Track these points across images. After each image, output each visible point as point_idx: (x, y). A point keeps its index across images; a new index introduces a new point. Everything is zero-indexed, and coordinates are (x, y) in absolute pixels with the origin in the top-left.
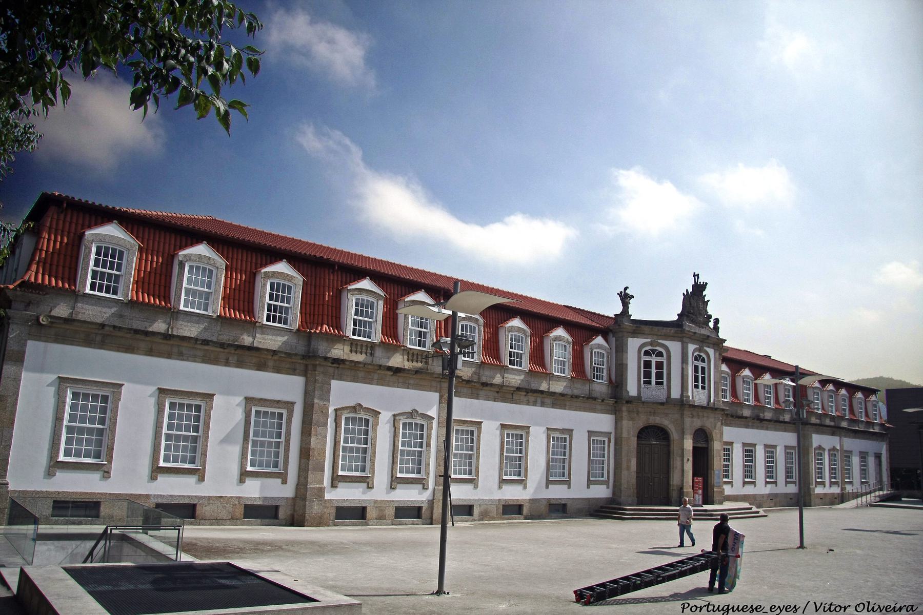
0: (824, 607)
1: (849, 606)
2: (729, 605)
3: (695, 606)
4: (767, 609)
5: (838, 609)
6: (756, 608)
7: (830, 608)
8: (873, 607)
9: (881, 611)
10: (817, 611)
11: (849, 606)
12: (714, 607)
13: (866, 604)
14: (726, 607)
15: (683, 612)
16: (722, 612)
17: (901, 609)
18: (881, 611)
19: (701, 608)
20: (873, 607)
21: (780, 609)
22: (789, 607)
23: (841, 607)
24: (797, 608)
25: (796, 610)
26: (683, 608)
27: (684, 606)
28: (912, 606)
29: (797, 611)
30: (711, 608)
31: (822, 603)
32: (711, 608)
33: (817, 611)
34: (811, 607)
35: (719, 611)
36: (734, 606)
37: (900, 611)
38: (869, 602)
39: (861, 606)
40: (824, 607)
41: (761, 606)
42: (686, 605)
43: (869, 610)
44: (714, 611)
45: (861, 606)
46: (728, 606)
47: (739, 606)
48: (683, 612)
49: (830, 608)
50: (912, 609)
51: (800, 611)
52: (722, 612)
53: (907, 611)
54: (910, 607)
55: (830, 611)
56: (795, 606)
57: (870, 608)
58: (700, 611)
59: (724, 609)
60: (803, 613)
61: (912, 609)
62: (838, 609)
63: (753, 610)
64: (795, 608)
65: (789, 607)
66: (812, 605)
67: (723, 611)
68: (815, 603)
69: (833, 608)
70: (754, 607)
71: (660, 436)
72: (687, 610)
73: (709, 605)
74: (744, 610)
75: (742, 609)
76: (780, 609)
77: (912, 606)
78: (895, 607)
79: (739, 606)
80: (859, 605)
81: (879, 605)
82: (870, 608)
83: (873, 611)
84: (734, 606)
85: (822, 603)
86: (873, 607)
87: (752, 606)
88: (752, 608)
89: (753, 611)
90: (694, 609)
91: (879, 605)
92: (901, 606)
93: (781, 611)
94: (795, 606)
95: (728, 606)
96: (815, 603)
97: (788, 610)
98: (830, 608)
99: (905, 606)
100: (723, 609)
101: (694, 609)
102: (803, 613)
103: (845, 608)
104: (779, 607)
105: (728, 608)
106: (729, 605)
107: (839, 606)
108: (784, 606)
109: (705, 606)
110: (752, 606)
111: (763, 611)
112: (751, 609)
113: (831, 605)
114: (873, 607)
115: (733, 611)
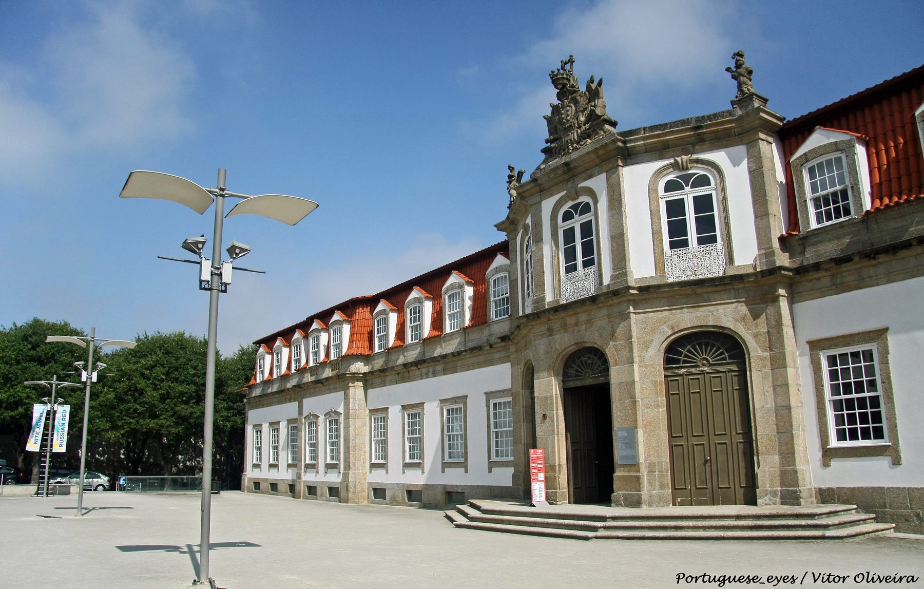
0: (823, 578)
1: (849, 576)
2: (725, 576)
3: (690, 576)
4: (764, 580)
5: (837, 579)
6: (753, 579)
7: (829, 578)
8: (873, 578)
9: (881, 582)
10: (815, 581)
11: (849, 576)
12: (710, 577)
13: (866, 575)
14: (722, 578)
15: (678, 583)
16: (718, 583)
17: (901, 579)
18: (881, 582)
19: (697, 579)
20: (873, 578)
21: (778, 579)
22: (786, 578)
23: (840, 578)
24: (795, 578)
25: (794, 581)
26: (679, 579)
27: (679, 576)
28: (913, 577)
29: (794, 582)
30: (706, 578)
31: (820, 574)
32: (706, 578)
33: (815, 581)
34: (809, 578)
35: (715, 582)
36: (730, 577)
37: (900, 582)
38: (868, 573)
39: (861, 576)
40: (823, 578)
41: (758, 577)
42: (682, 576)
43: (869, 580)
44: (709, 582)
45: (861, 576)
46: (725, 576)
47: (735, 576)
48: (678, 583)
49: (828, 579)
50: (912, 579)
51: (798, 581)
52: (718, 583)
53: (908, 582)
54: (910, 578)
55: (829, 582)
56: (793, 576)
57: (870, 579)
58: (696, 582)
59: (721, 580)
60: (801, 584)
61: (912, 579)
62: (837, 579)
63: (750, 580)
64: (793, 579)
65: (786, 578)
66: (809, 576)
67: (720, 581)
68: (813, 573)
69: (831, 578)
70: (750, 578)
71: (686, 356)
72: (683, 581)
73: (705, 575)
74: (741, 581)
75: (739, 580)
76: (778, 579)
77: (913, 577)
78: (895, 578)
80: (858, 575)
81: (878, 576)
82: (870, 579)
83: (873, 582)
84: (730, 577)
85: (820, 574)
86: (873, 578)
87: (749, 576)
88: (749, 579)
89: (750, 582)
90: (689, 579)
91: (878, 576)
92: (901, 577)
93: (778, 582)
94: (793, 576)
95: (725, 576)
96: (813, 573)
97: (785, 581)
98: (828, 579)
99: (906, 576)
100: (719, 580)
101: (689, 579)
102: (801, 584)
103: (844, 579)
104: (776, 577)
105: (724, 579)
106: (725, 576)
107: (838, 576)
108: (781, 577)
109: (701, 576)
110: (749, 576)
111: (760, 581)
112: (748, 580)
113: (830, 575)
114: (873, 578)
115: (730, 582)
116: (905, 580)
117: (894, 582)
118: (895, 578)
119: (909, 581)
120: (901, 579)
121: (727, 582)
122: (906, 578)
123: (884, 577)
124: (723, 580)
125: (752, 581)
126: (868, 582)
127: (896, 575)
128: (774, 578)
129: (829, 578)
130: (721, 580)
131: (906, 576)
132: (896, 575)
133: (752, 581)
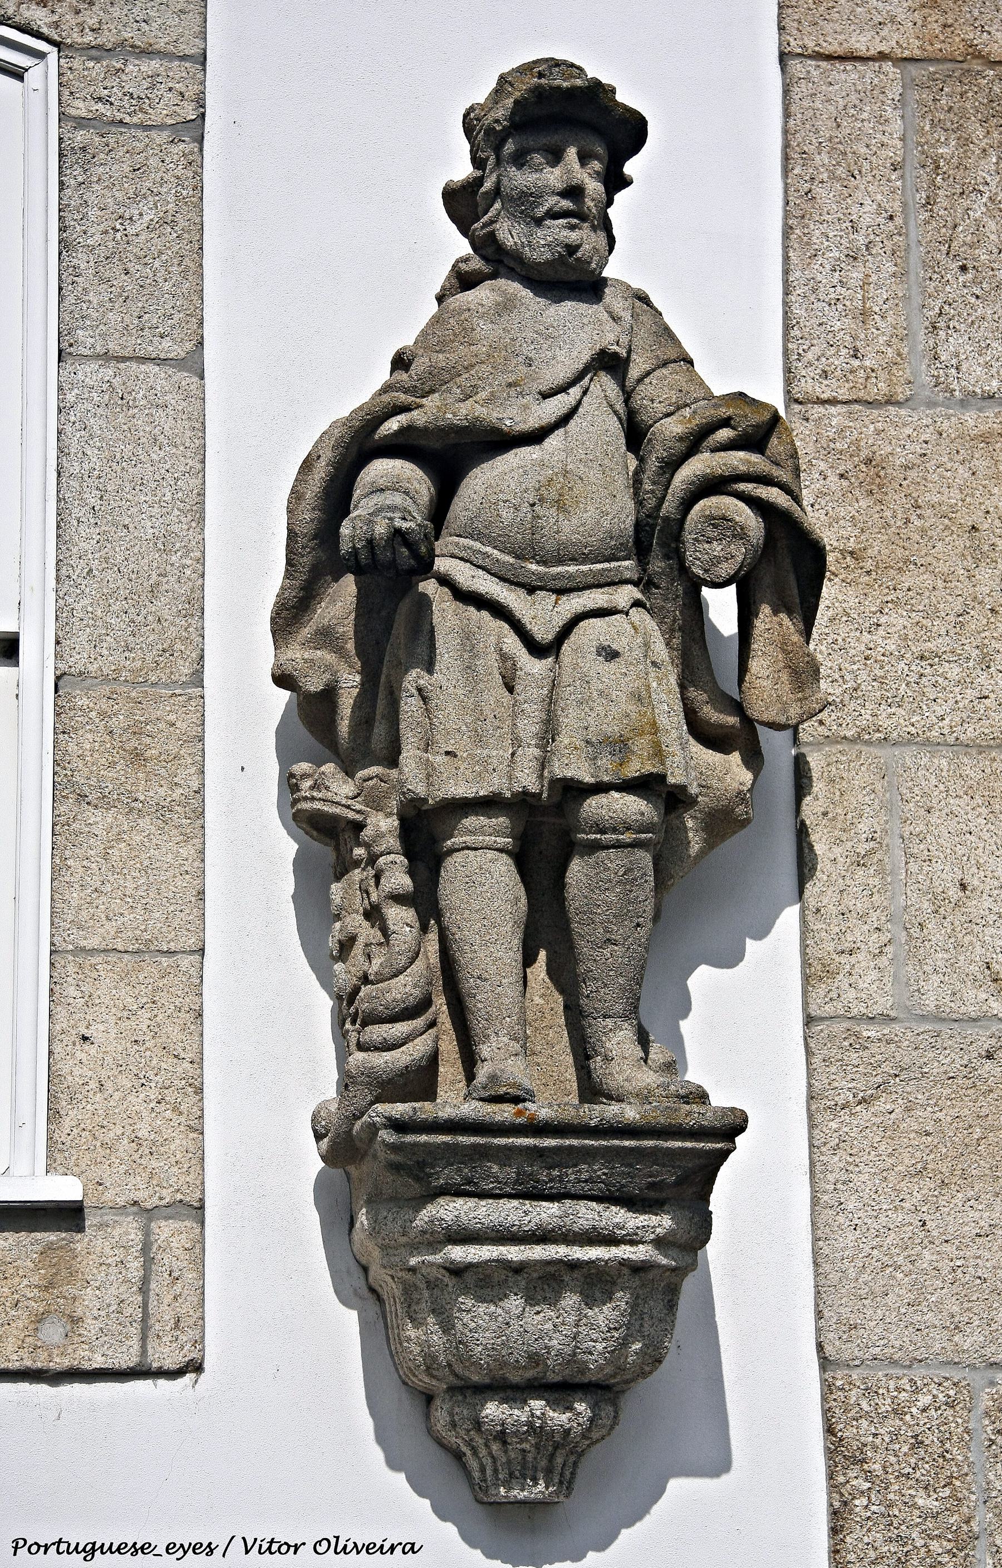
0: (261, 1546)
1: (304, 1544)
2: (95, 1542)
4: (161, 1550)
5: (284, 1549)
7: (272, 1547)
9: (358, 1553)
10: (247, 1552)
11: (304, 1544)
12: (69, 1545)
13: (333, 1541)
17: (392, 1548)
18: (358, 1553)
20: (345, 1546)
23: (289, 1546)
24: (213, 1547)
25: (212, 1551)
33: (247, 1552)
34: (238, 1545)
36: (103, 1544)
37: (392, 1553)
38: (337, 1538)
39: (325, 1543)
40: (261, 1546)
41: (150, 1545)
45: (325, 1543)
46: (94, 1544)
47: (78, 1544)
49: (269, 1548)
50: (412, 1548)
51: (218, 1552)
53: (404, 1553)
56: (210, 1543)
59: (87, 1550)
61: (412, 1548)
62: (284, 1549)
63: (136, 1551)
64: (210, 1548)
67: (85, 1552)
70: (138, 1546)
74: (122, 1551)
75: (118, 1550)
77: (413, 1544)
78: (382, 1546)
79: (78, 1544)
80: (320, 1542)
81: (355, 1543)
83: (345, 1553)
84: (103, 1544)
86: (345, 1546)
87: (135, 1543)
88: (135, 1548)
91: (355, 1543)
92: (393, 1545)
93: (185, 1552)
94: (210, 1543)
95: (94, 1544)
98: (269, 1548)
99: (400, 1544)
100: (84, 1550)
103: (297, 1548)
104: (182, 1546)
105: (93, 1548)
106: (95, 1542)
107: (286, 1543)
110: (135, 1543)
112: (133, 1550)
113: (272, 1542)
115: (102, 1553)
116: (399, 1548)
117: (382, 1553)
118: (382, 1546)
119: (406, 1551)
120: (392, 1548)
121: (98, 1553)
122: (400, 1548)
123: (364, 1545)
124: (91, 1551)
125: (140, 1551)
126: (336, 1553)
127: (383, 1541)
128: (178, 1546)
129: (272, 1547)
130: (87, 1550)
131: (400, 1544)
132: (383, 1541)
133: (140, 1551)
